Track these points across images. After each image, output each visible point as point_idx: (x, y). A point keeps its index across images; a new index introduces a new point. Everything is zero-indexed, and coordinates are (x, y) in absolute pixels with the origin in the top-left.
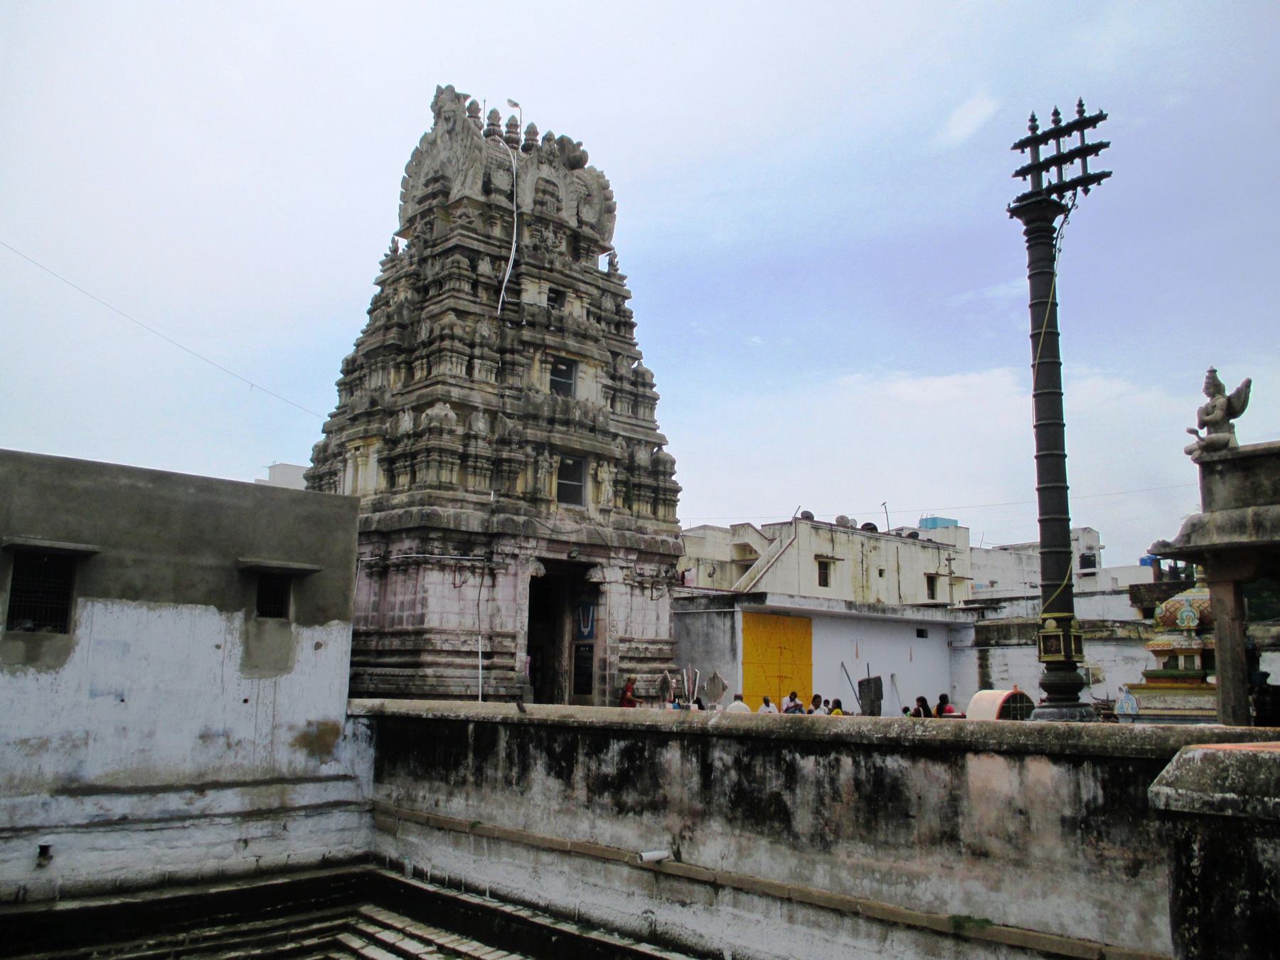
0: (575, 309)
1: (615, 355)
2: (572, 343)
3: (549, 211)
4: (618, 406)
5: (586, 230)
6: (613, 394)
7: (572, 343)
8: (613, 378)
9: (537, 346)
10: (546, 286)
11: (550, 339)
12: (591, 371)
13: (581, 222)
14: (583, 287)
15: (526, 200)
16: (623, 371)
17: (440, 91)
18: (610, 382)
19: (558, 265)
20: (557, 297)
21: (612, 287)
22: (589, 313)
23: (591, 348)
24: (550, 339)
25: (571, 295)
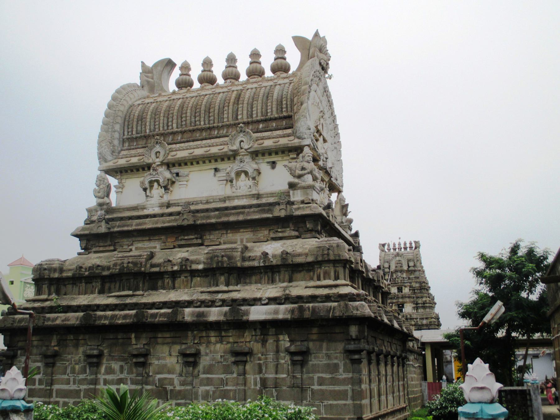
0: (406, 290)
1: (417, 297)
2: (401, 300)
3: (399, 268)
4: (419, 311)
5: (410, 269)
6: (416, 308)
7: (401, 300)
8: (417, 304)
9: (392, 303)
10: (396, 288)
11: (394, 301)
12: (408, 305)
13: (409, 267)
14: (406, 284)
15: (393, 268)
16: (420, 301)
17: (380, 244)
18: (414, 306)
19: (399, 281)
20: (400, 290)
21: (418, 280)
22: (410, 290)
23: (407, 300)
24: (394, 301)
25: (403, 288)
